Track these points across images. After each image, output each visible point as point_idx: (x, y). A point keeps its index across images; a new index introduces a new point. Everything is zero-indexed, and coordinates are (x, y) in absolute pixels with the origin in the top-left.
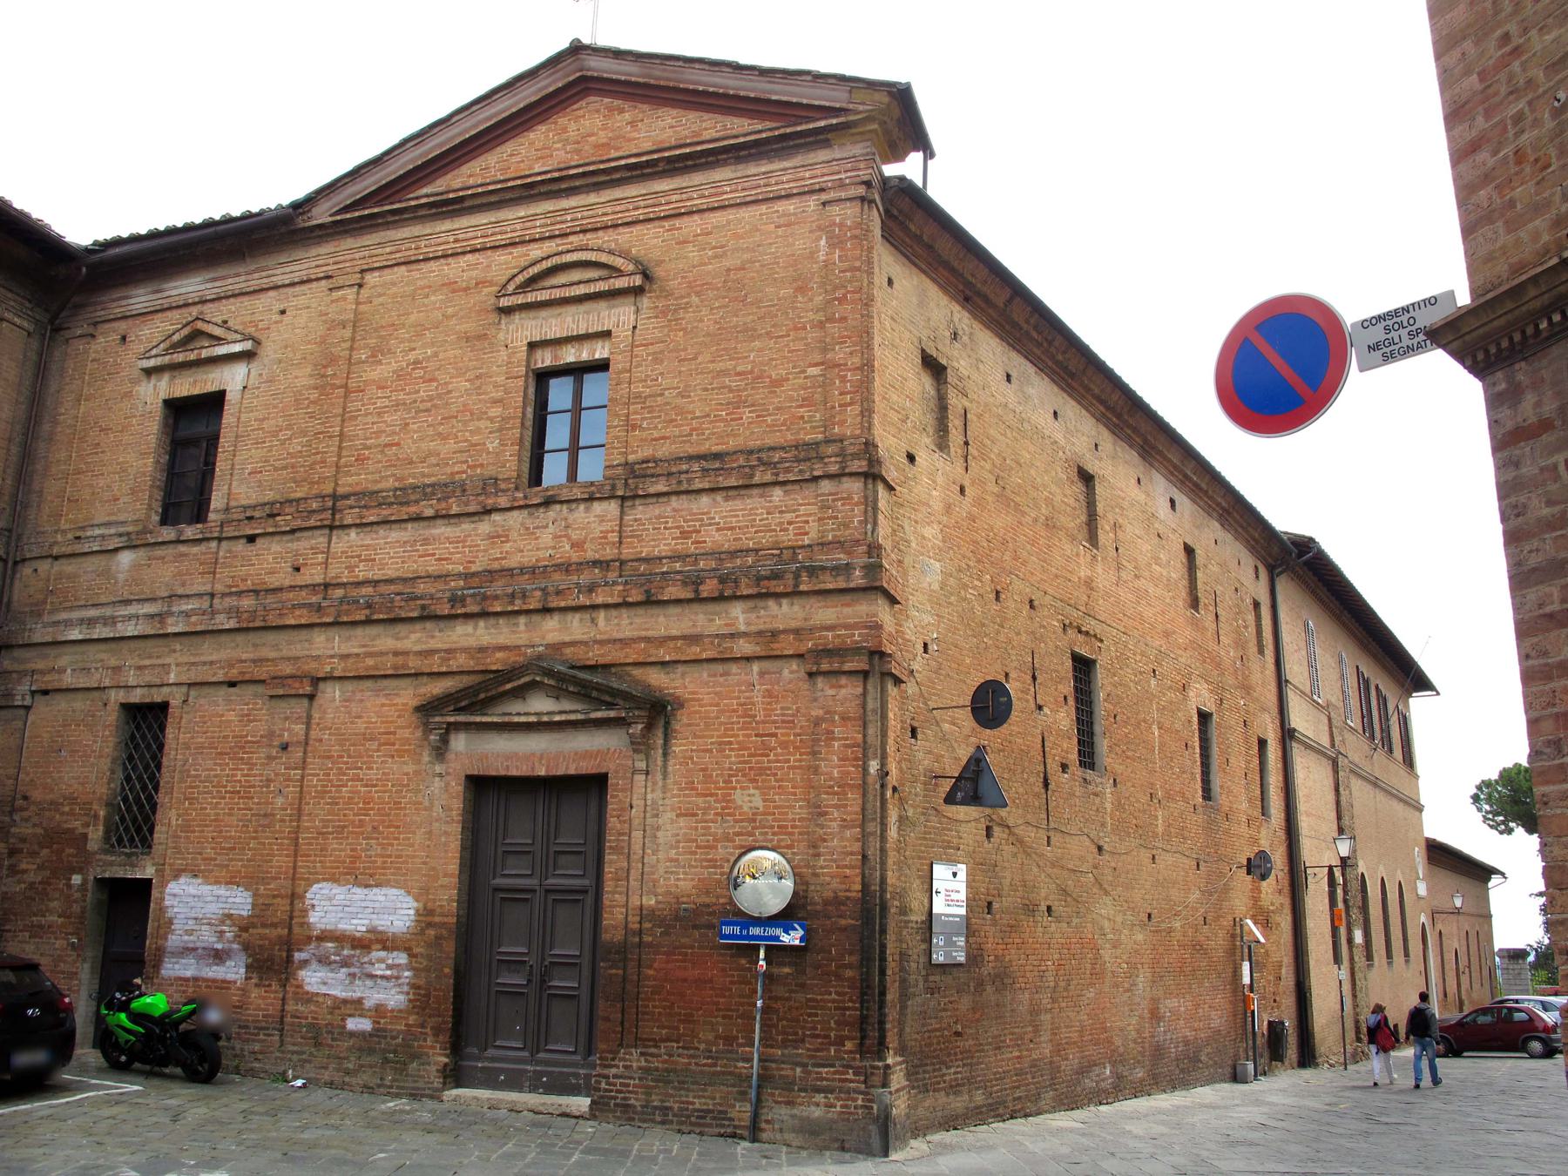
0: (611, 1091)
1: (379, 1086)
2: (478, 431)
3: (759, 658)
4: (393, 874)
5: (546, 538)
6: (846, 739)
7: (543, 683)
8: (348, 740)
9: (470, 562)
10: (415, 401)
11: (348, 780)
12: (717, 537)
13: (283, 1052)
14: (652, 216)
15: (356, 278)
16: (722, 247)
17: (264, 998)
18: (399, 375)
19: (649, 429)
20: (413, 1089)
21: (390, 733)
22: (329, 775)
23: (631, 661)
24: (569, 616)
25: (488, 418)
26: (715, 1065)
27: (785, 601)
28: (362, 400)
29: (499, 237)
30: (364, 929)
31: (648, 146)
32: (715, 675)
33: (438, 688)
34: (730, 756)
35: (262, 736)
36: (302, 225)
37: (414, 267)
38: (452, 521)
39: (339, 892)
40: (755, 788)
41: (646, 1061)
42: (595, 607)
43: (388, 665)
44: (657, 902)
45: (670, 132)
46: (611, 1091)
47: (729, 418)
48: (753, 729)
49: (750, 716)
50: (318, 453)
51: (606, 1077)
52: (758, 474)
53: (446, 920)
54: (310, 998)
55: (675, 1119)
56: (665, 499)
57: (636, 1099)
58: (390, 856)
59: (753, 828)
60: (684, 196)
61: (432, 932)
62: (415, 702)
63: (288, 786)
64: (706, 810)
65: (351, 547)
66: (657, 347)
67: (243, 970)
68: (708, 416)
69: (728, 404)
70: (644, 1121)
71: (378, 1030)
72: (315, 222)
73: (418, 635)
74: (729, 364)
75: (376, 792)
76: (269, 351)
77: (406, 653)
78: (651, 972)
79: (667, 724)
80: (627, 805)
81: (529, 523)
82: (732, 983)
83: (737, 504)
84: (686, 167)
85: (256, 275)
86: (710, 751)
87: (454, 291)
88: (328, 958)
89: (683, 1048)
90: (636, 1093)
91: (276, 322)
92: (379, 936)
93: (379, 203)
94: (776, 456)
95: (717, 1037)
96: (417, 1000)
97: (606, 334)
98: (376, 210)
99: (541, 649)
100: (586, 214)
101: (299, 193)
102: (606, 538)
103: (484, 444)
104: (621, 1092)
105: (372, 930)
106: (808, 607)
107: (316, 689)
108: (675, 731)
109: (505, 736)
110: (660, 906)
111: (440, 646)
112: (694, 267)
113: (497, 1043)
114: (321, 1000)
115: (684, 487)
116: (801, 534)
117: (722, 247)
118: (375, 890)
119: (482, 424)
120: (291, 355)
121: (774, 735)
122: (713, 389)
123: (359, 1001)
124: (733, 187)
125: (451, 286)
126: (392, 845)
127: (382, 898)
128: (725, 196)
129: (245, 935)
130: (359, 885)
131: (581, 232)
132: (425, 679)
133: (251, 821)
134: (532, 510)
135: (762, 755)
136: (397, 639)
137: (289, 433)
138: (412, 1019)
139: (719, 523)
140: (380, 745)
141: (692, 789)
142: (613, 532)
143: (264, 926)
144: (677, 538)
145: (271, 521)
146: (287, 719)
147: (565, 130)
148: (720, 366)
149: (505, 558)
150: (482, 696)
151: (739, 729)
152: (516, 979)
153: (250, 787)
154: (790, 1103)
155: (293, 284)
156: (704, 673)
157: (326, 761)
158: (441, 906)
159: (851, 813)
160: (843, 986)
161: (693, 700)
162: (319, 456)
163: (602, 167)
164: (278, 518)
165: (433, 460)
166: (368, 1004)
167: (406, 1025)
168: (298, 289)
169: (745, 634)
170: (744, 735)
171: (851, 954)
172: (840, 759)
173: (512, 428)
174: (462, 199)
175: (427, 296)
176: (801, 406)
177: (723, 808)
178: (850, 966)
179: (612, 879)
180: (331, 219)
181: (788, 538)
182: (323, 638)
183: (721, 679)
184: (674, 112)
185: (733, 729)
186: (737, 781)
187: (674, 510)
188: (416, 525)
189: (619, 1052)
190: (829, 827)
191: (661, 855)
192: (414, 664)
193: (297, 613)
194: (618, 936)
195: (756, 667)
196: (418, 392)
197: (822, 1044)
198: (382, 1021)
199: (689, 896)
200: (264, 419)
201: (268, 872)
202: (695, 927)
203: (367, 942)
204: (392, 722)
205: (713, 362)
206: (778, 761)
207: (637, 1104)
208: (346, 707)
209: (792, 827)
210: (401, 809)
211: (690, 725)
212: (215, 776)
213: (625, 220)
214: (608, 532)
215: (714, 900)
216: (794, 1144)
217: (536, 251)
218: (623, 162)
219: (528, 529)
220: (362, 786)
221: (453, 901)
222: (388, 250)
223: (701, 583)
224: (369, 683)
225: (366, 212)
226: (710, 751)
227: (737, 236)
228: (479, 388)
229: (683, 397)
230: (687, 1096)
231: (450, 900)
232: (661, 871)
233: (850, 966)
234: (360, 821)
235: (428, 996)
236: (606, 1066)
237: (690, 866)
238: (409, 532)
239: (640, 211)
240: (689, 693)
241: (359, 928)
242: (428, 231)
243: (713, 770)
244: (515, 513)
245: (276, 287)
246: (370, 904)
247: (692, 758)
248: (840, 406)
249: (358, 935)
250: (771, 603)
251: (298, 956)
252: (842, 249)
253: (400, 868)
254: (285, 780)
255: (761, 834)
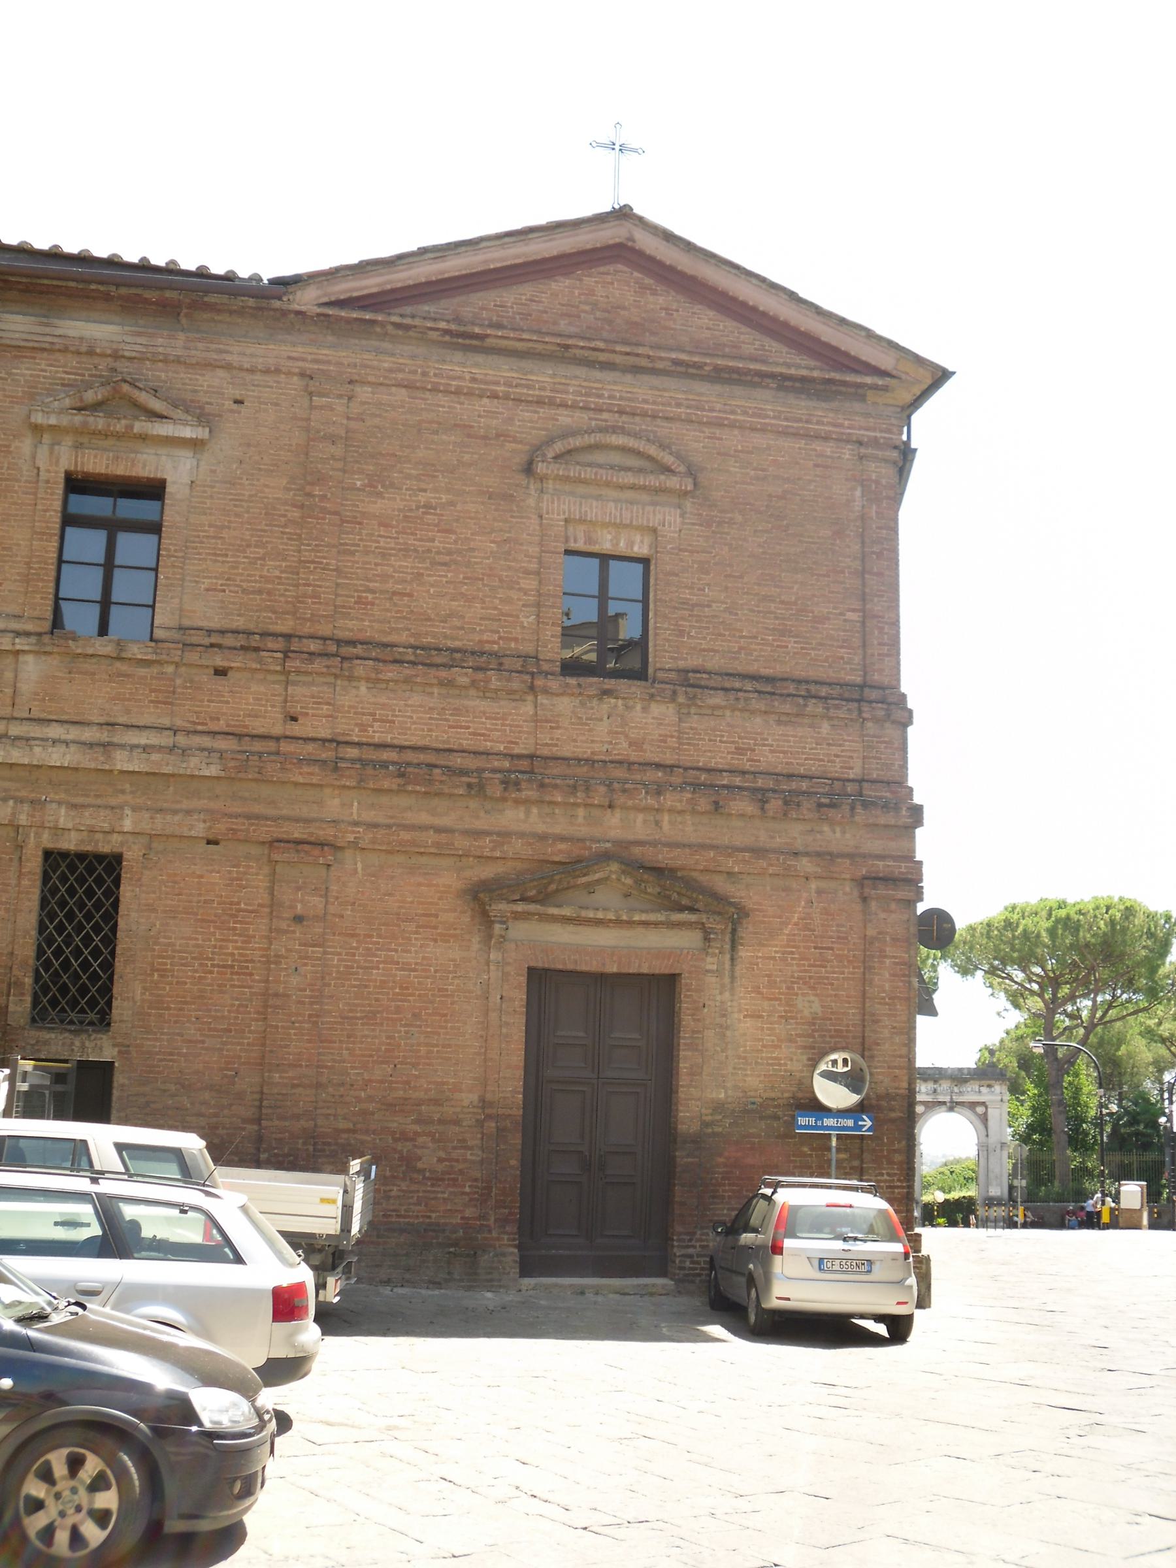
0: (696, 1269)
2: (507, 601)
5: (603, 728)
9: (512, 743)
10: (429, 551)
12: (771, 758)
33: (487, 872)
35: (259, 905)
46: (696, 1269)
48: (813, 942)
50: (309, 585)
51: (691, 1256)
53: (509, 1112)
58: (437, 1046)
63: (305, 965)
65: (362, 702)
68: (756, 637)
72: (296, 307)
75: (415, 977)
78: (721, 1160)
80: (701, 1005)
86: (774, 958)
99: (608, 845)
102: (665, 742)
103: (518, 617)
108: (742, 938)
116: (846, 768)
117: (763, 470)
121: (832, 949)
122: (759, 612)
126: (439, 1034)
128: (767, 421)
137: (261, 551)
139: (772, 746)
142: (672, 737)
143: (282, 1118)
144: (732, 753)
146: (299, 889)
149: (556, 745)
153: (247, 961)
160: (893, 1169)
161: (757, 910)
165: (456, 622)
168: (258, 377)
170: (805, 947)
172: (891, 975)
173: (553, 607)
177: (785, 1011)
181: (835, 769)
184: (711, 313)
186: (799, 988)
189: (695, 1233)
194: (694, 1128)
196: (433, 540)
198: (434, 1215)
200: (223, 527)
202: (761, 1118)
204: (431, 903)
206: (834, 973)
211: (756, 933)
214: (666, 736)
215: (780, 1095)
219: (580, 718)
221: (519, 1093)
229: (731, 613)
234: (398, 1007)
235: (489, 1188)
254: (300, 958)
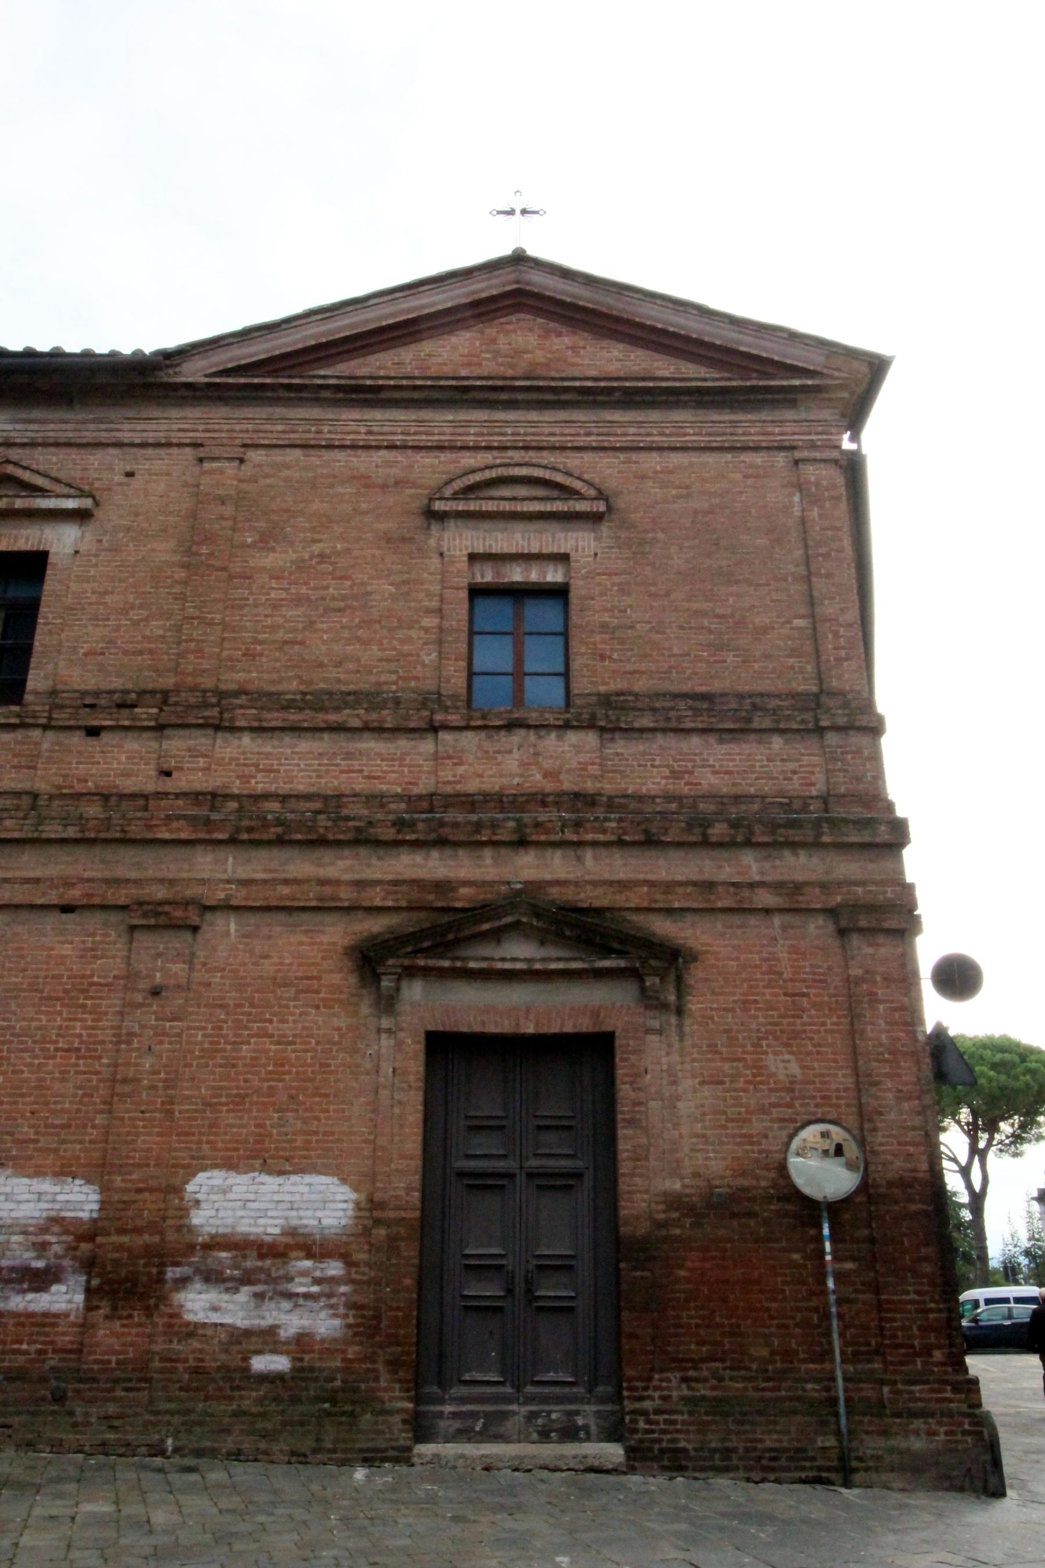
0: (653, 1432)
1: (315, 1451)
2: (409, 640)
3: (781, 911)
4: (319, 1157)
5: (512, 763)
6: (892, 1002)
7: (532, 926)
8: (249, 985)
9: (411, 783)
10: (323, 598)
11: (252, 1036)
12: (713, 780)
13: (156, 1413)
14: (606, 444)
15: (238, 452)
16: (687, 488)
17: (118, 1336)
18: (300, 565)
19: (621, 661)
20: (368, 1450)
21: (313, 978)
22: (221, 1028)
23: (632, 905)
24: (549, 852)
25: (422, 628)
26: (779, 1389)
27: (802, 853)
28: (249, 588)
29: (424, 437)
30: (277, 1231)
31: (593, 373)
32: (731, 927)
33: (376, 925)
34: (757, 1017)
35: (115, 977)
36: (165, 379)
37: (312, 452)
38: (385, 735)
39: (240, 1183)
40: (790, 1053)
41: (689, 1388)
42: (580, 844)
43: (310, 896)
44: (685, 1186)
45: (618, 365)
46: (653, 1432)
47: (712, 659)
48: (780, 987)
49: (776, 973)
50: (192, 640)
51: (644, 1413)
52: (756, 719)
53: (403, 1214)
54: (193, 1330)
55: (741, 1464)
56: (650, 736)
57: (688, 1441)
58: (316, 1133)
59: (792, 1099)
60: (642, 431)
61: (382, 1232)
62: (347, 942)
63: (161, 1042)
64: (734, 1078)
65: (244, 753)
66: (624, 578)
67: (79, 1298)
68: (688, 655)
69: (709, 645)
70: (703, 1469)
71: (302, 1370)
72: (183, 379)
73: (348, 862)
74: (706, 606)
75: (294, 1051)
76: (110, 516)
77: (337, 882)
78: (682, 1273)
79: (679, 979)
80: (642, 1069)
81: (487, 745)
82: (784, 1283)
83: (734, 748)
84: (644, 402)
85: (92, 426)
86: (733, 1010)
87: (367, 486)
88: (221, 1273)
89: (732, 1368)
90: (688, 1432)
91: (120, 484)
92: (300, 1239)
93: (274, 373)
94: (774, 703)
95: (773, 1353)
96: (358, 1325)
97: (564, 558)
98: (268, 381)
99: (519, 886)
100: (529, 430)
101: (171, 341)
102: (586, 770)
103: (418, 655)
104: (663, 1432)
105: (291, 1232)
106: (828, 860)
107: (202, 920)
108: (690, 986)
109: (477, 985)
110: (688, 1191)
111: (378, 876)
112: (657, 503)
113: (467, 1377)
114: (209, 1332)
115: (673, 724)
116: (807, 785)
117: (687, 488)
118: (294, 1178)
119: (414, 633)
120: (145, 525)
121: (804, 995)
122: (690, 628)
123: (271, 1331)
124: (697, 430)
125: (365, 482)
126: (318, 1119)
127: (305, 1189)
128: (687, 438)
129: (85, 1247)
130: (270, 1173)
131: (522, 448)
132: (360, 914)
133: (97, 1088)
134: (492, 732)
135: (793, 1016)
136: (319, 865)
137: (145, 613)
138: (352, 1352)
139: (713, 766)
140: (298, 992)
141: (716, 1052)
142: (593, 764)
143: (121, 1231)
144: (666, 778)
145: (125, 712)
146: (159, 955)
147: (494, 341)
148: (695, 606)
149: (459, 782)
150: (451, 936)
151: (764, 987)
152: (488, 1290)
153: (94, 1043)
154: (885, 1433)
155: (143, 445)
156: (719, 923)
157: (219, 1011)
158: (397, 1197)
159: (907, 1084)
160: (922, 1284)
161: (707, 952)
162: (193, 645)
163: (553, 384)
164: (137, 710)
165: (351, 666)
166: (283, 1334)
167: (344, 1360)
168: (150, 451)
169: (762, 884)
170: (771, 994)
171: (927, 1245)
172: (887, 1023)
173: (456, 641)
174: (380, 388)
175: (332, 486)
176: (790, 656)
177: (754, 1075)
178: (926, 1259)
179: (630, 1159)
180: (207, 380)
181: (794, 786)
182: (209, 858)
183: (739, 932)
184: (621, 346)
185: (757, 986)
186: (768, 1045)
187: (662, 748)
188: (335, 736)
189: (650, 1379)
190: (884, 1098)
191: (685, 1130)
192: (346, 895)
193: (175, 824)
194: (642, 1229)
195: (777, 920)
196: (327, 588)
197: (904, 1355)
198: (307, 1357)
199: (722, 1177)
200: (106, 593)
201: (128, 1157)
202: (734, 1215)
203: (281, 1249)
204: (314, 964)
205: (689, 601)
206: (811, 1024)
207: (690, 1447)
208: (247, 944)
209: (838, 1098)
210: (331, 1072)
211: (706, 980)
212: (39, 1028)
213: (576, 444)
214: (587, 763)
215: (754, 1183)
216: (894, 1485)
217: (469, 460)
218: (577, 384)
219: (487, 752)
220: (271, 1043)
221: (413, 1189)
222: (280, 428)
223: (709, 826)
224: (281, 917)
225: (256, 381)
226: (733, 1010)
227: (704, 480)
228: (408, 594)
229: (658, 632)
230: (754, 1432)
231: (409, 1190)
232: (686, 1150)
233: (926, 1259)
234: (270, 1088)
235: (377, 1317)
236: (641, 1399)
237: (721, 1143)
238: (325, 743)
239: (593, 438)
240: (703, 945)
241: (270, 1230)
242: (330, 416)
243: (739, 1032)
244: (470, 734)
245: (119, 445)
246: (288, 1197)
247: (712, 1018)
248: (836, 659)
249: (268, 1239)
250: (787, 853)
251: (172, 1273)
252: (821, 507)
253: (332, 1149)
254: (156, 1035)
255: (801, 1105)
